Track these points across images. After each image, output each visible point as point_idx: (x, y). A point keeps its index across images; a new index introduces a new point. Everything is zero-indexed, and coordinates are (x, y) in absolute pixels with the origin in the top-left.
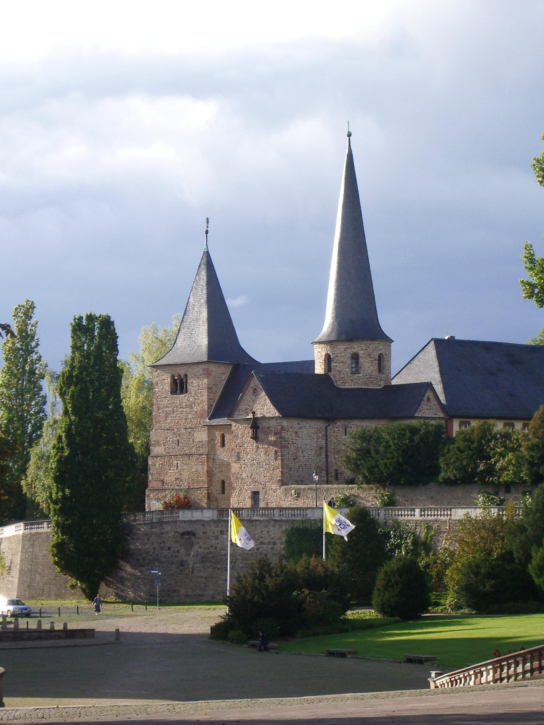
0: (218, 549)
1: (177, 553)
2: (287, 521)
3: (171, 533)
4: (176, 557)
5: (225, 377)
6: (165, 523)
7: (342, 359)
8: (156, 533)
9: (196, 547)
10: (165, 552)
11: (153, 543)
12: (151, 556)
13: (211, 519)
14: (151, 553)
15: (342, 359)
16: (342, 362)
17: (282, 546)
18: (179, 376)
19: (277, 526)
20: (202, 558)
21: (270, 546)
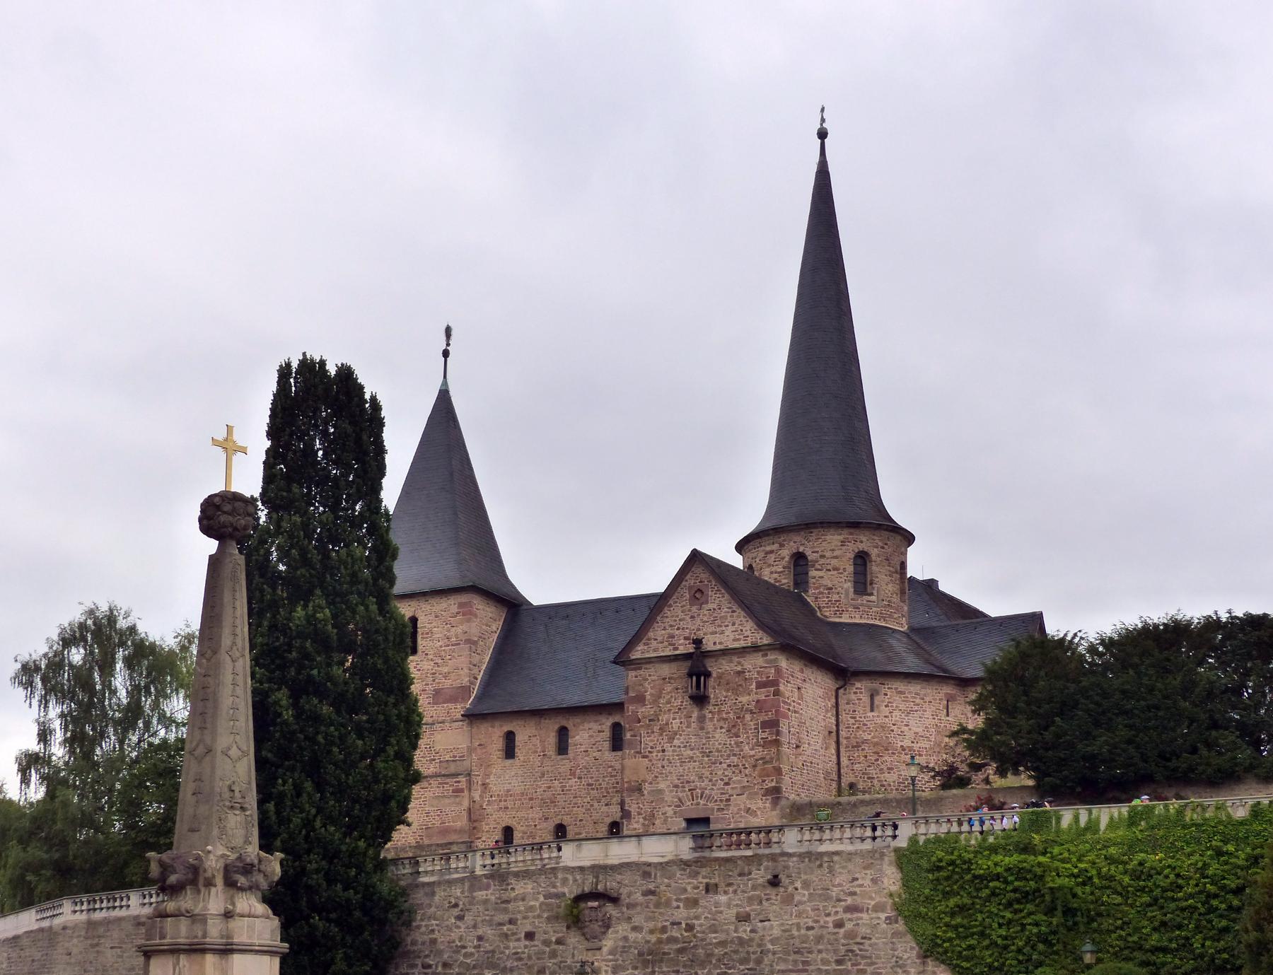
1: (554, 947)
3: (537, 899)
4: (553, 954)
5: (497, 626)
7: (834, 562)
8: (486, 902)
9: (620, 930)
11: (475, 927)
12: (466, 955)
15: (834, 562)
16: (835, 569)
20: (640, 954)
21: (883, 916)
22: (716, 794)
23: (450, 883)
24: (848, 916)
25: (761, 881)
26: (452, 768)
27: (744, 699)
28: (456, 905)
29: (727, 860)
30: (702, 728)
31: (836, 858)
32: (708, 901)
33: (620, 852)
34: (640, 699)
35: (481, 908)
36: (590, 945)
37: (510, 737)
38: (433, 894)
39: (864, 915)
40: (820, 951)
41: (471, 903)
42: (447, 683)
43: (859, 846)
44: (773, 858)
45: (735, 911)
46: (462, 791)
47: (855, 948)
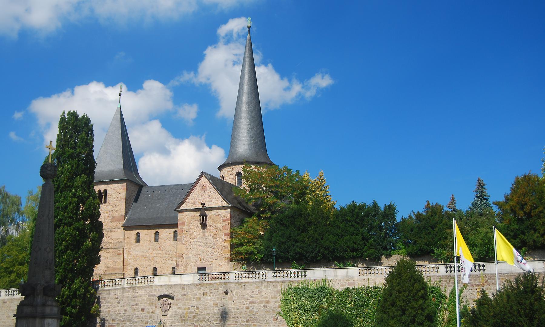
0: (200, 308)
1: (151, 314)
2: (282, 282)
3: (145, 297)
4: (151, 317)
6: (139, 287)
8: (128, 297)
10: (139, 313)
11: (124, 306)
12: (120, 317)
13: (191, 282)
14: (121, 315)
17: (277, 304)
18: (100, 191)
19: (271, 287)
20: (181, 317)
22: (208, 259)
23: (115, 289)
24: (251, 305)
25: (222, 292)
26: (118, 246)
27: (218, 225)
28: (117, 298)
29: (211, 284)
30: (204, 235)
31: (247, 284)
32: (203, 298)
33: (175, 280)
34: (183, 224)
35: (126, 299)
36: (163, 314)
37: (138, 234)
38: (110, 294)
39: (256, 305)
40: (241, 318)
41: (123, 298)
42: (117, 214)
43: (254, 280)
44: (226, 283)
45: (213, 302)
46: (121, 254)
47: (253, 316)
